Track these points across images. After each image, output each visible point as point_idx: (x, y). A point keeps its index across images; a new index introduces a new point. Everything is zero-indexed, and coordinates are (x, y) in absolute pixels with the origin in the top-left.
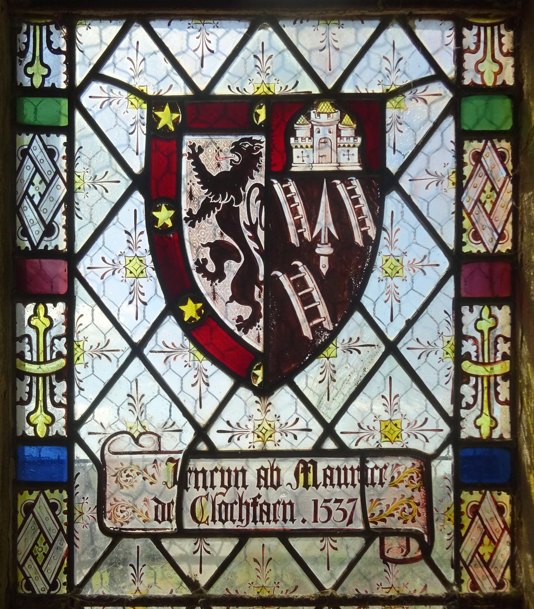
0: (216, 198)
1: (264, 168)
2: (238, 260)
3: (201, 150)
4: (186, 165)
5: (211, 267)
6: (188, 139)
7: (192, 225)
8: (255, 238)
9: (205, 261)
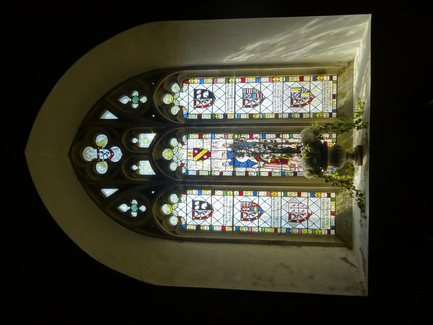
2: (254, 100)
5: (255, 102)
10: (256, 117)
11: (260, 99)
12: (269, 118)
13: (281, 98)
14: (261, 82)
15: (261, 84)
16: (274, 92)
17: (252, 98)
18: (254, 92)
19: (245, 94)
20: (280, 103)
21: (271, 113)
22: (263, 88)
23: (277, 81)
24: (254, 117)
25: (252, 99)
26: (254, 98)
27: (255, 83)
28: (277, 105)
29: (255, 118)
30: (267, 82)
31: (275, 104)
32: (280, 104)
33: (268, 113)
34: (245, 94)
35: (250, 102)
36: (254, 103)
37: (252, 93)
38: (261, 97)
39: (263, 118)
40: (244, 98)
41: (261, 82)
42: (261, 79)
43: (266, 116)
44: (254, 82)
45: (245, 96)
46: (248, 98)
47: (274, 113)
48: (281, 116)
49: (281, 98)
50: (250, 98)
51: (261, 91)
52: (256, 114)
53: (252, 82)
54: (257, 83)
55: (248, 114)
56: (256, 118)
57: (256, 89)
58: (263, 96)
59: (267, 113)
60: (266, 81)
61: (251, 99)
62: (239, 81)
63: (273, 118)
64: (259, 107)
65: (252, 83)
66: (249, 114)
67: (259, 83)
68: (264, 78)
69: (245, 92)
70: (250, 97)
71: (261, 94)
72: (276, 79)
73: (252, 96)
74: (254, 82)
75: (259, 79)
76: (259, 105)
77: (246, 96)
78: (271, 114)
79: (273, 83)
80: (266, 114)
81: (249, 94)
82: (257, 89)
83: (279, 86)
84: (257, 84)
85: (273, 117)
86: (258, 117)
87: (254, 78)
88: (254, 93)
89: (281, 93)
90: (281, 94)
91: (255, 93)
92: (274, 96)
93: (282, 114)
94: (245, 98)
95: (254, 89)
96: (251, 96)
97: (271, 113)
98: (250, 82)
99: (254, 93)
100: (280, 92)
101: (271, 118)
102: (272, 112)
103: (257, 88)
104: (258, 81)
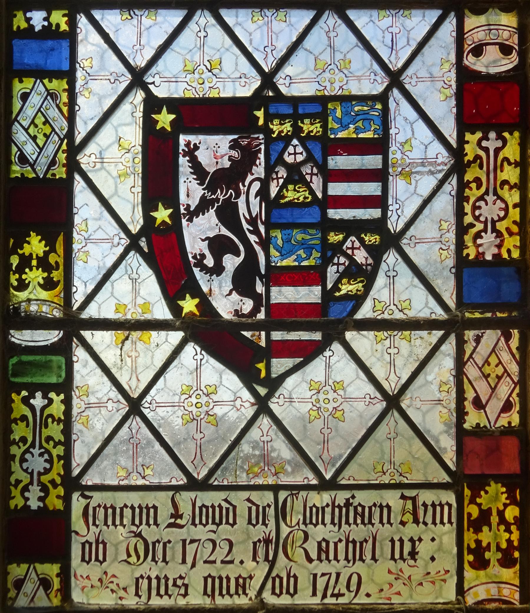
0: (214, 193)
1: (263, 164)
2: (238, 254)
3: (196, 147)
4: (183, 161)
5: (210, 262)
6: (183, 139)
7: (190, 220)
8: (256, 232)
9: (203, 256)
10: (20, 270)
11: (257, 326)
12: (16, 436)
13: (252, 593)
14: (470, 335)
15: (439, 334)
16: (342, 497)
17: (269, 225)
18: (338, 248)
19: (316, 128)
20: (202, 570)
21: (67, 457)
22: (392, 363)
23: (469, 538)
24: (27, 250)
25: (253, 221)
26: (257, 248)
27: (451, 262)
28: (176, 535)
29: (15, 261)
30: (468, 406)
31: (185, 509)
32: (183, 570)
33: (77, 427)
34: (316, 128)
35: (212, 188)
36: (204, 247)
37: (334, 214)
38: (276, 336)
39: (14, 360)
40: (269, 118)
41: (470, 335)
42: (508, 337)
43: (38, 401)
44: (468, 239)
45: (287, 127)
46: (270, 169)
47: (67, 500)
48: (29, 587)
49: (256, 584)
50: (263, 193)
51: (349, 335)
52: (57, 275)
53: (468, 219)
54: (452, 283)
55: (61, 173)
56: (14, 279)
57: (383, 266)
58: (288, 363)
59: (68, 412)
60: (470, 395)
61: (255, 202)
62: (478, 51)
63: (9, 497)
64: (147, 306)
65: (460, 213)
66: (69, 182)
67: (451, 303)
68: (514, 368)
69: (345, 127)
70: (274, 190)
71: (317, 336)
72: (495, 519)
73: (287, 216)
74: (460, 245)
75: (502, 307)
76: (176, 310)
77: (286, 140)
78: (58, 468)
79: (445, 478)
80: (57, 398)
81: (317, 184)
82: (381, 280)
83: (413, 554)
84: (438, 284)
85: (16, 492)
86: (23, 295)
87: (516, 240)
88: (334, 238)
89: (321, 583)
90: (304, 583)
91: (326, 261)
92: (282, 495)
93: (56, 602)
94: (267, 131)
95: (372, 239)
96: (291, 204)
97: (67, 467)
98: (473, 193)
99: (325, 244)
100: (331, 568)
101: (15, 466)
102: (89, 480)
103: (392, 278)
104: (476, 298)
